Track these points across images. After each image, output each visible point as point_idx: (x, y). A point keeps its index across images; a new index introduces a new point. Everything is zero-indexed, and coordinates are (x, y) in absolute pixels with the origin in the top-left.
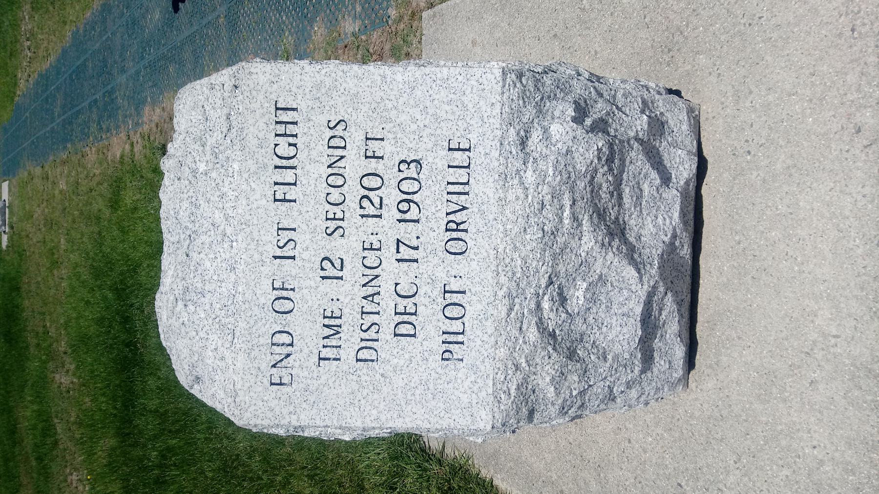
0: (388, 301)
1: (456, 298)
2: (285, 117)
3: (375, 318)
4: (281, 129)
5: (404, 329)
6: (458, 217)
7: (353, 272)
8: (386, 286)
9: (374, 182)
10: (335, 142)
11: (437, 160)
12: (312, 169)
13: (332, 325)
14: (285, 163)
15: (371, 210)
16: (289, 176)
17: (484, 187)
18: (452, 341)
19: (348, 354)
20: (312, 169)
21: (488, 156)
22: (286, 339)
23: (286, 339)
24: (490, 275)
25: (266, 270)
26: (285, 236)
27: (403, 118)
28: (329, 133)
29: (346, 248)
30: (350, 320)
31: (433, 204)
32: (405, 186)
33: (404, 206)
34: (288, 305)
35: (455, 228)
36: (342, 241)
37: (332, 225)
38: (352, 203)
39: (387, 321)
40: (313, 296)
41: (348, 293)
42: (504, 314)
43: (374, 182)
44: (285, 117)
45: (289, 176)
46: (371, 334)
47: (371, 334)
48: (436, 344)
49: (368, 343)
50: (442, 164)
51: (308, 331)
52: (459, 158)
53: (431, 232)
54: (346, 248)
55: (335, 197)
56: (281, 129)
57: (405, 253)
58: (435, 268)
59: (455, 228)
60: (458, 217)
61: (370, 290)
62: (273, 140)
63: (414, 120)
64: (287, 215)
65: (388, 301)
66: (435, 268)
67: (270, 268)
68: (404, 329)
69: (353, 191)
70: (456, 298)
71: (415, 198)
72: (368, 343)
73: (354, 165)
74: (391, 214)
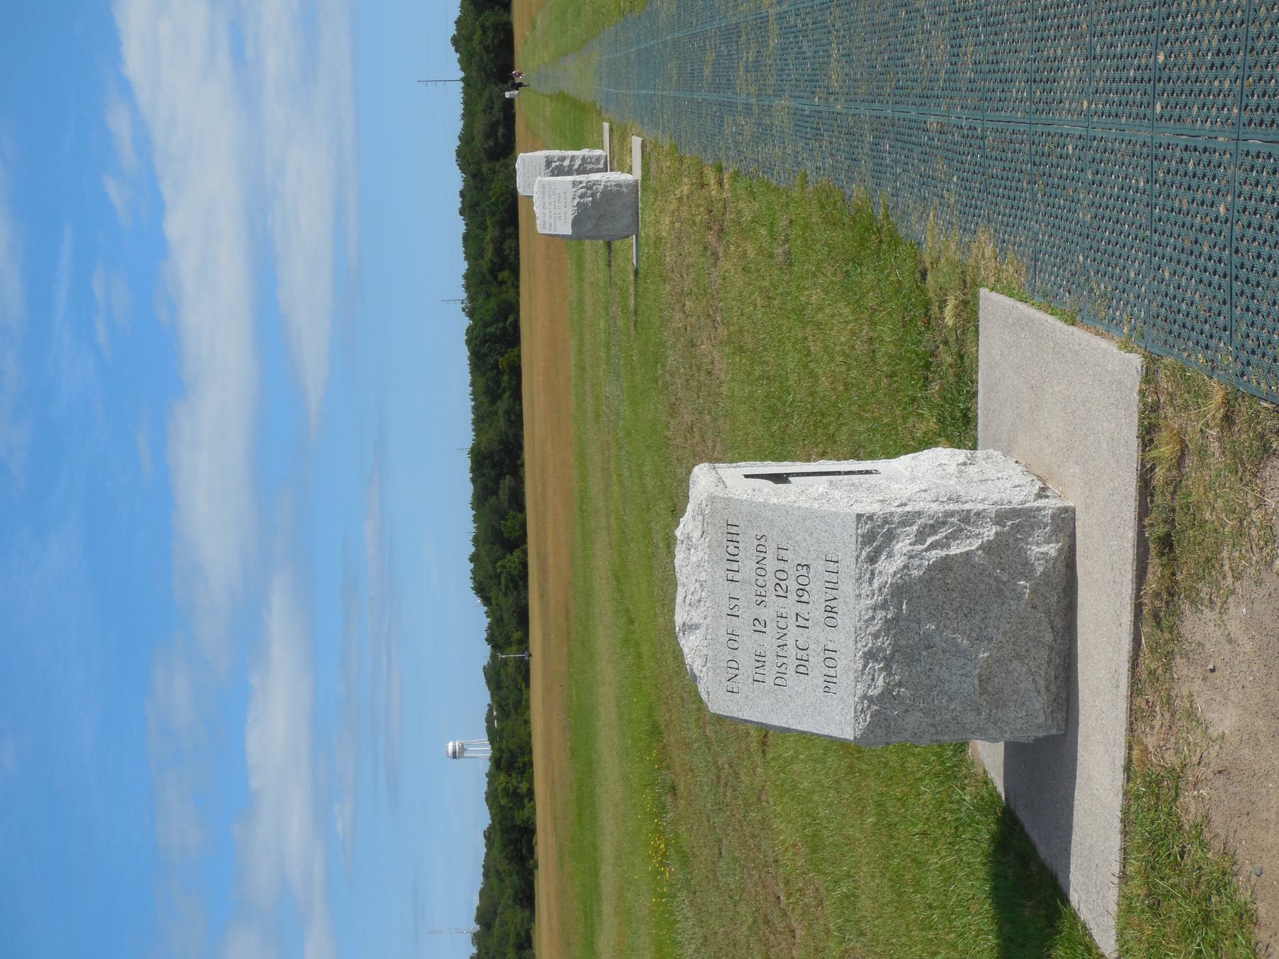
0: (792, 651)
1: (831, 654)
2: (734, 530)
3: (785, 660)
4: (730, 537)
5: (801, 669)
6: (832, 604)
7: (771, 629)
8: (790, 641)
9: (783, 576)
10: (760, 548)
11: (818, 566)
12: (747, 567)
13: (760, 659)
14: (733, 558)
15: (781, 593)
16: (735, 566)
17: (847, 587)
18: (829, 680)
19: (770, 679)
20: (747, 567)
21: (849, 568)
22: (734, 665)
23: (734, 665)
24: (851, 643)
25: (723, 621)
26: (735, 602)
27: (799, 538)
28: (757, 543)
29: (767, 613)
30: (770, 658)
31: (817, 594)
32: (801, 580)
33: (800, 593)
34: (736, 645)
35: (830, 610)
36: (764, 610)
37: (760, 599)
38: (770, 585)
39: (792, 663)
40: (749, 642)
41: (768, 642)
42: (860, 667)
43: (783, 576)
44: (734, 530)
45: (735, 566)
46: (782, 669)
47: (782, 669)
48: (820, 681)
49: (781, 674)
50: (821, 569)
51: (746, 660)
52: (832, 566)
53: (816, 612)
54: (767, 613)
55: (761, 582)
56: (730, 537)
57: (801, 622)
58: (818, 636)
59: (830, 610)
60: (832, 604)
61: (781, 642)
62: (726, 543)
63: (805, 540)
64: (736, 590)
65: (792, 651)
66: (818, 636)
67: (725, 620)
68: (801, 669)
69: (771, 580)
70: (831, 654)
71: (807, 588)
72: (781, 674)
73: (771, 564)
74: (793, 597)
